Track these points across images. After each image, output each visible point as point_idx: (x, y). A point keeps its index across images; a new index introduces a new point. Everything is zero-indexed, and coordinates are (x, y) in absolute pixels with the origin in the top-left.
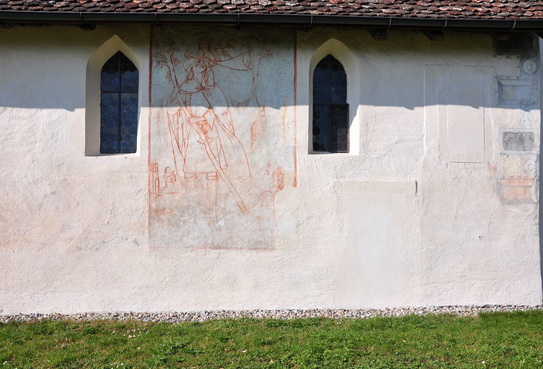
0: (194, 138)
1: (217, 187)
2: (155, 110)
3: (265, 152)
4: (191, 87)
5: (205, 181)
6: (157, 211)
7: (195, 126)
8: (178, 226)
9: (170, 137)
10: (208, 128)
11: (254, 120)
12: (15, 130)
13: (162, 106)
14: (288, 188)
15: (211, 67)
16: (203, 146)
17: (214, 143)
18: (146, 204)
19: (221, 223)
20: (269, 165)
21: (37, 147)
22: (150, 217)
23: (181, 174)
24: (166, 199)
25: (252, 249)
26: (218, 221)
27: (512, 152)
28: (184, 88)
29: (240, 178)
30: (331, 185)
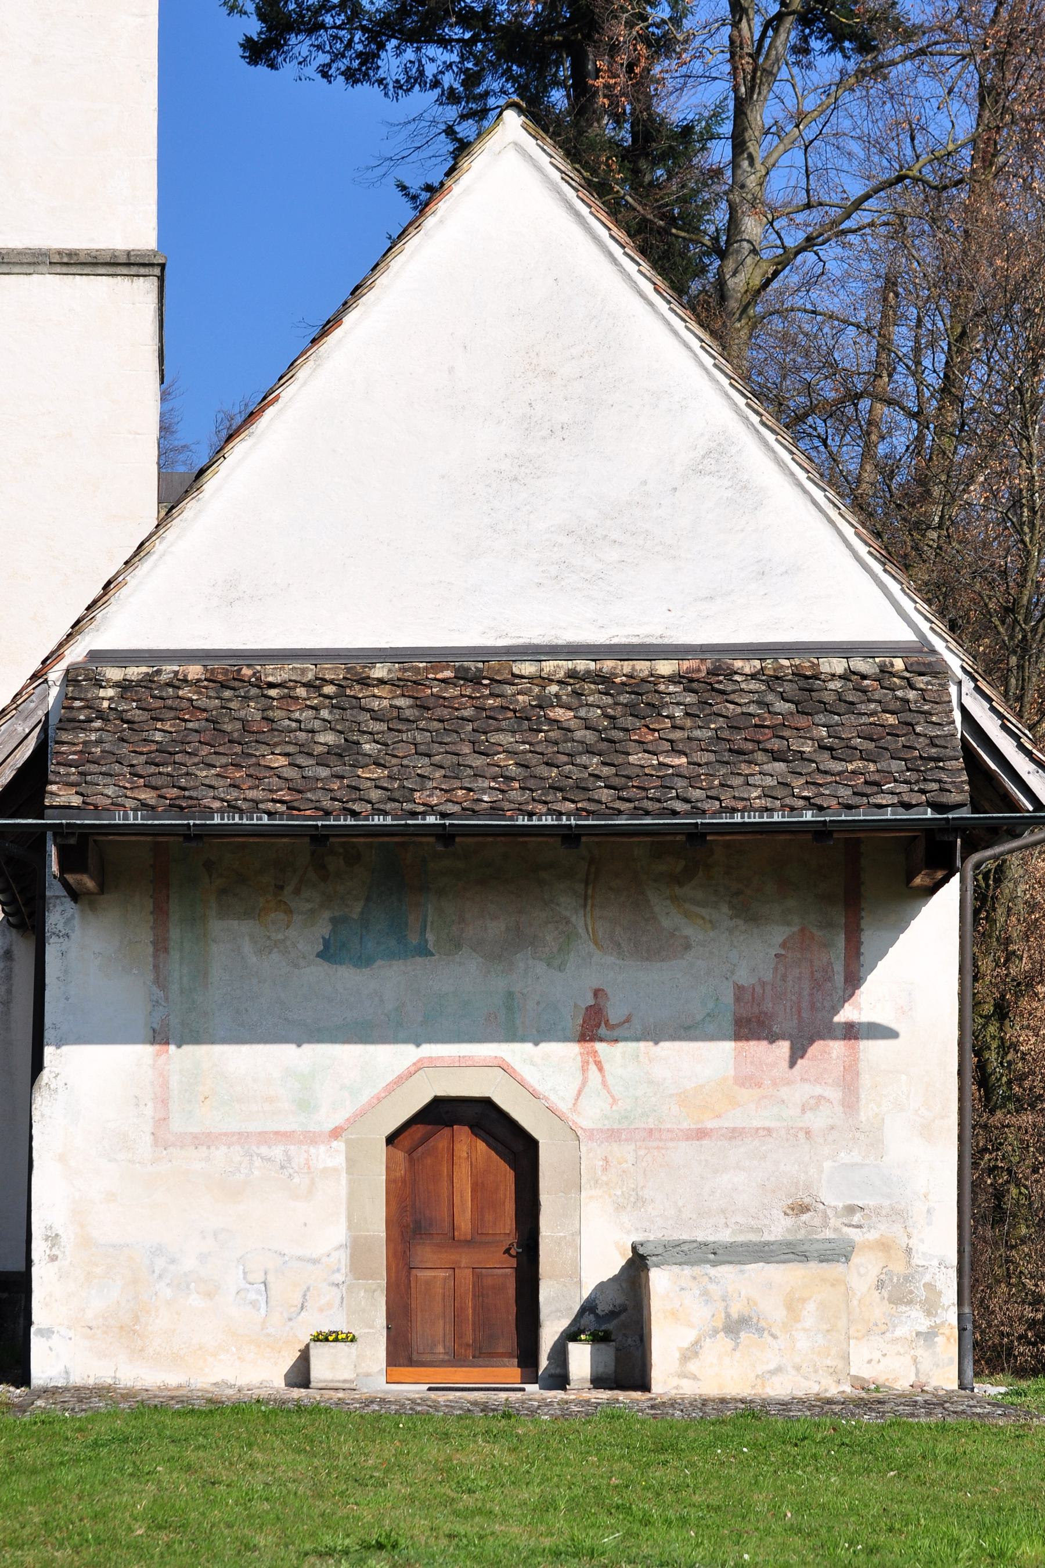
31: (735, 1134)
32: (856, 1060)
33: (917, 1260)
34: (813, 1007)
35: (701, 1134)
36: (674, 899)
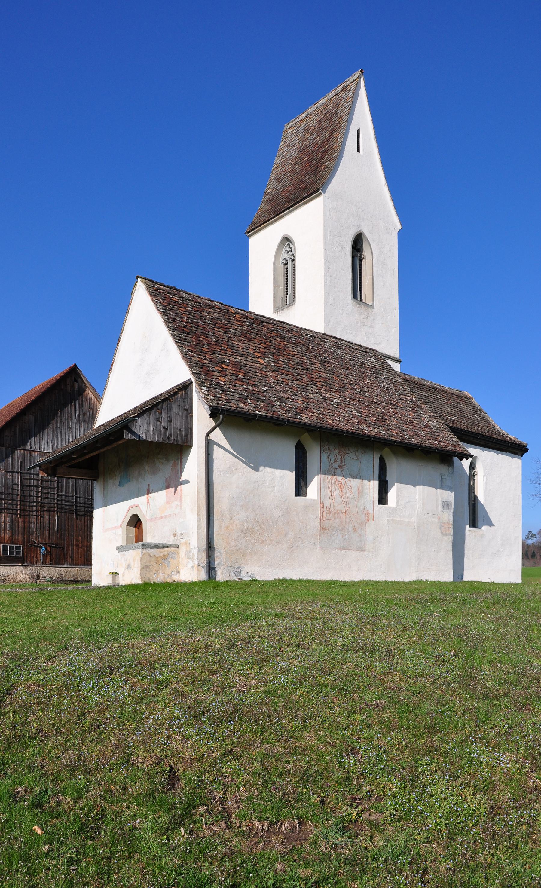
0: (338, 492)
1: (346, 518)
2: (323, 476)
3: (363, 502)
4: (336, 465)
5: (341, 515)
6: (323, 528)
7: (337, 485)
9: (328, 491)
10: (342, 488)
11: (359, 485)
12: (266, 479)
13: (325, 474)
14: (371, 521)
15: (344, 456)
16: (340, 496)
17: (345, 495)
19: (347, 536)
20: (364, 508)
21: (276, 490)
23: (333, 510)
25: (357, 550)
27: (445, 510)
28: (333, 465)
29: (354, 514)
30: (386, 521)
31: (166, 517)
32: (182, 494)
33: (191, 547)
34: (176, 481)
35: (162, 518)
36: (158, 459)
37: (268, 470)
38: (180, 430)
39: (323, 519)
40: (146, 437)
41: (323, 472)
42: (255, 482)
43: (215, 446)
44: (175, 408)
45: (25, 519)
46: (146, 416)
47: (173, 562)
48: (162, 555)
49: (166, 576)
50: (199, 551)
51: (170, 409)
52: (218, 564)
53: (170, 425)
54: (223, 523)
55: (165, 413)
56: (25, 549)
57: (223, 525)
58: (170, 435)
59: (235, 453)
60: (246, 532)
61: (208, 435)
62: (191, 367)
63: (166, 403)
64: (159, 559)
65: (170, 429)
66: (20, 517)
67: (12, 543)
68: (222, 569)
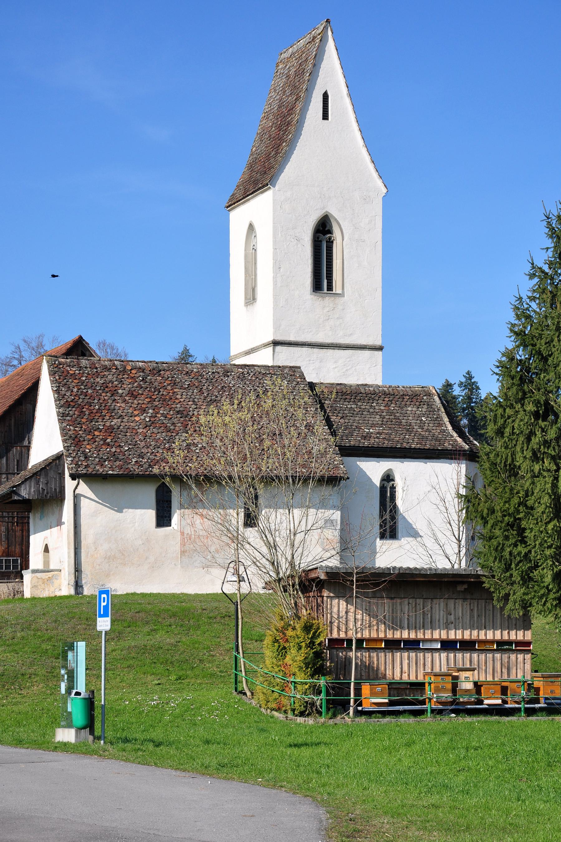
6: (184, 552)
8: (192, 558)
18: (179, 549)
22: (181, 554)
24: (187, 547)
26: (207, 556)
37: (130, 510)
38: (55, 489)
39: (183, 544)
40: (29, 497)
41: (182, 507)
42: (117, 521)
43: (82, 498)
44: (52, 474)
45: (23, 527)
46: (28, 482)
47: (56, 582)
48: (47, 577)
49: (51, 593)
50: (69, 574)
51: (46, 475)
52: (85, 583)
53: (47, 486)
54: (89, 553)
55: (43, 478)
56: (24, 562)
57: (89, 554)
58: (48, 493)
59: (101, 501)
60: (109, 558)
61: (74, 491)
62: (64, 441)
63: (43, 472)
64: (45, 580)
65: (47, 489)
66: (17, 525)
67: (8, 555)
68: (88, 586)
